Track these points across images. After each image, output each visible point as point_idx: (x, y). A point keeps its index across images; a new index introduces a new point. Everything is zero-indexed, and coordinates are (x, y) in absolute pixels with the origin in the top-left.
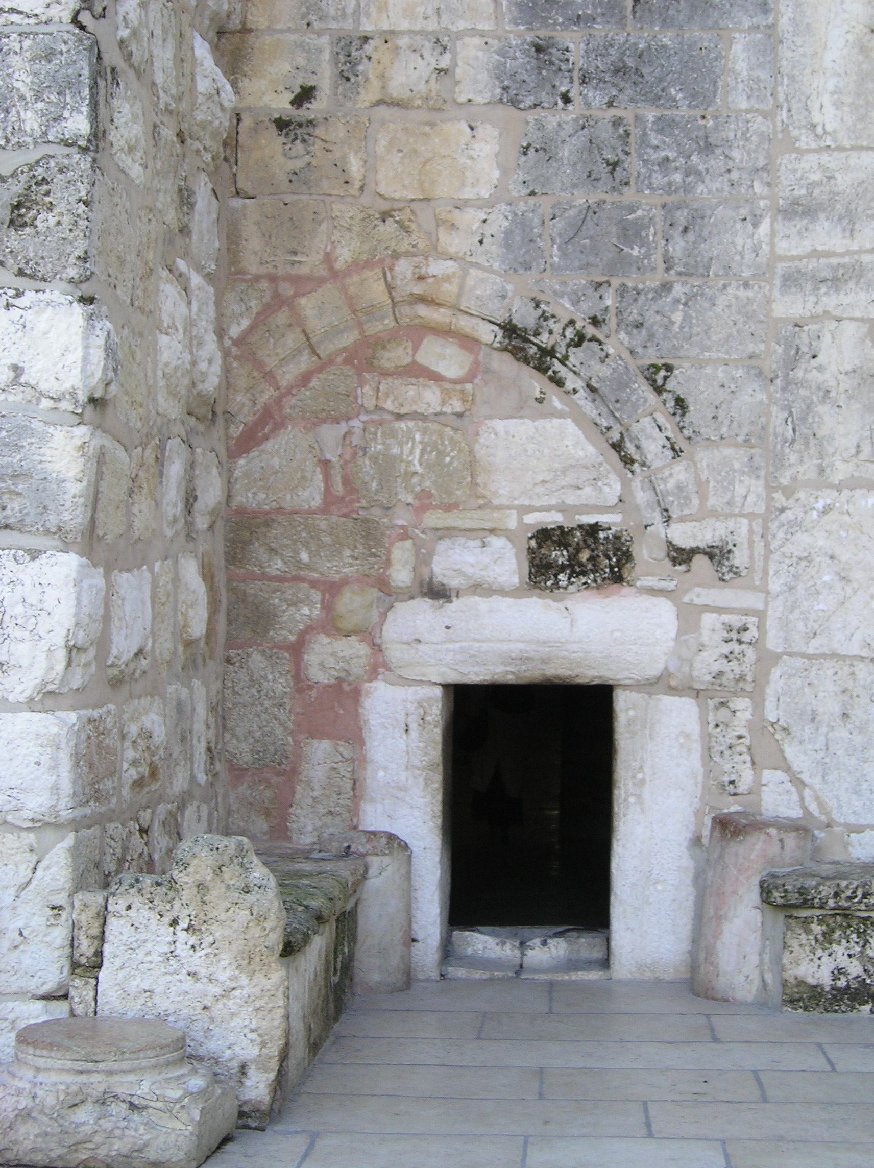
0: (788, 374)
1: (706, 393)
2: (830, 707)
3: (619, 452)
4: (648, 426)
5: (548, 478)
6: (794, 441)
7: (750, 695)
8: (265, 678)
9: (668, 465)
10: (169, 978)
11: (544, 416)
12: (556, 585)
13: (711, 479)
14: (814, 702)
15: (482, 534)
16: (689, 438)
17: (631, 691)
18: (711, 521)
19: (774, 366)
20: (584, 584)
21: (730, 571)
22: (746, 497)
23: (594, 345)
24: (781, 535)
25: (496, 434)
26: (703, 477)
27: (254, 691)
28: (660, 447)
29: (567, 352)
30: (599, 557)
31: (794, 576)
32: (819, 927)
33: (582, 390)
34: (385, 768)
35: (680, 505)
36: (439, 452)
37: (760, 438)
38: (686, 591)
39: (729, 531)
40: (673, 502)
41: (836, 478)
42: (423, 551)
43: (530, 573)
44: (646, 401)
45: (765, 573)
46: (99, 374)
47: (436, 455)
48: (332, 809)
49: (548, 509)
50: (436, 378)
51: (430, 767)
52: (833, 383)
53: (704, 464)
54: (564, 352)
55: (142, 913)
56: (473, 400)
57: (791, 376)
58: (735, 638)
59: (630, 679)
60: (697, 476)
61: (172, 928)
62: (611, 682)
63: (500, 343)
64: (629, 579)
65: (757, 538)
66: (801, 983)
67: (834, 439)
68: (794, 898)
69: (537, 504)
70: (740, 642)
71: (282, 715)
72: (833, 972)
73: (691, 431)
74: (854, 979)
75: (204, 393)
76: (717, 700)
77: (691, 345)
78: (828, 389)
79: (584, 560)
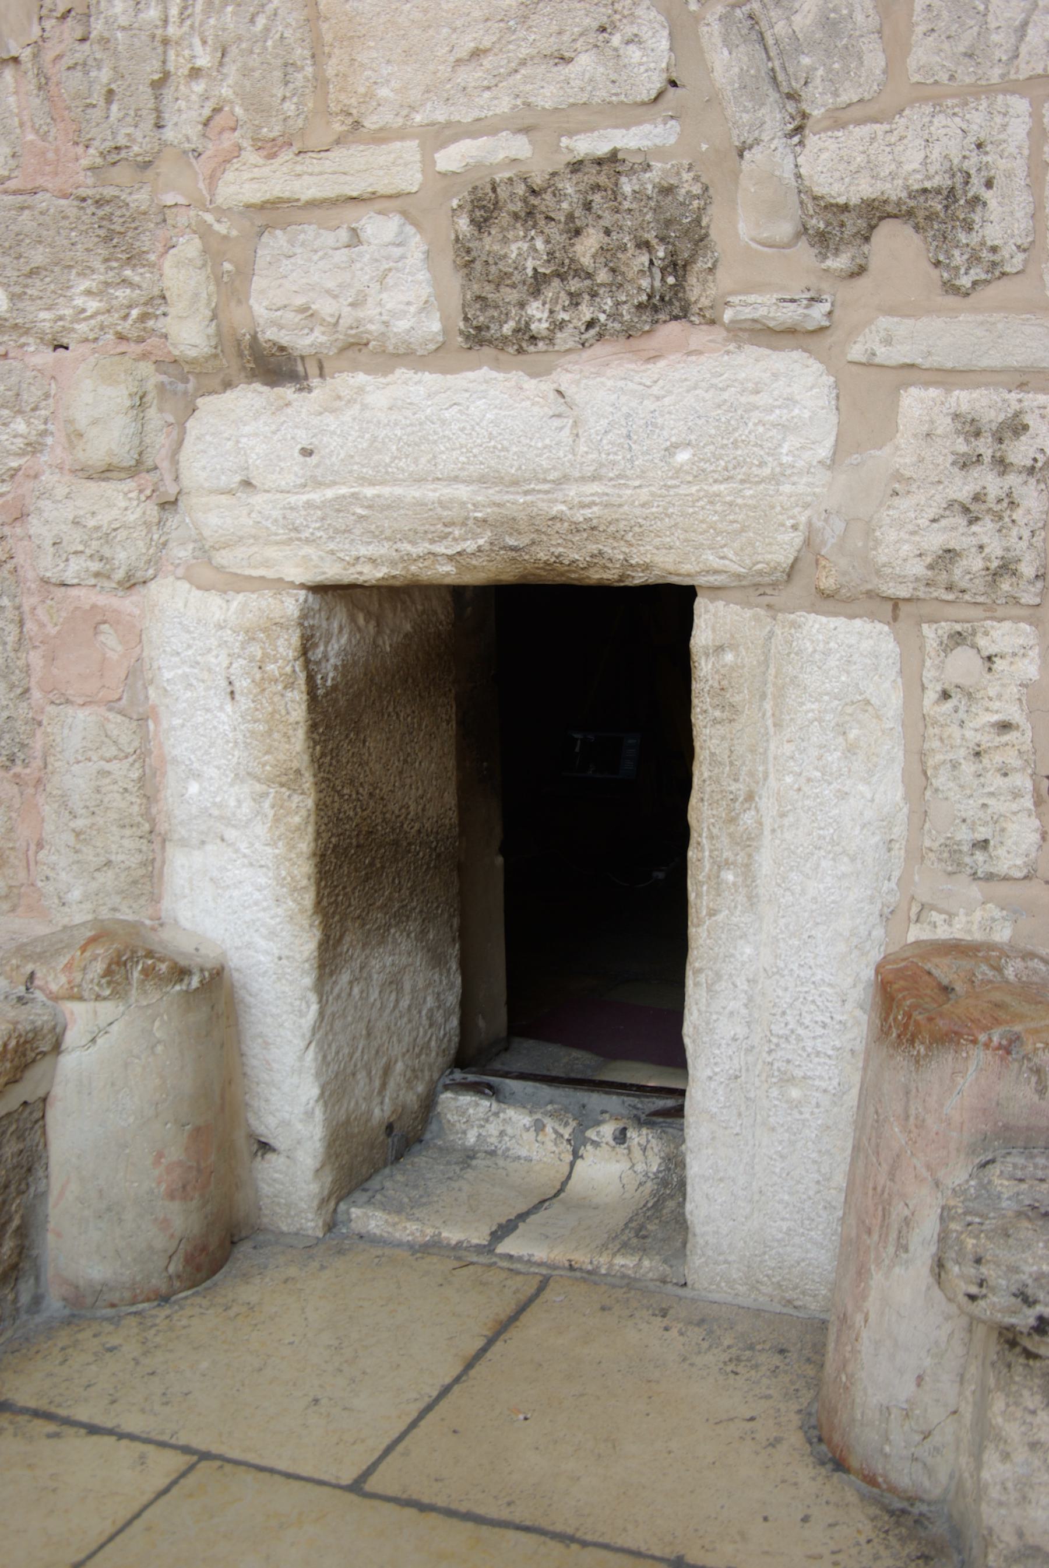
5: (486, 43)
15: (350, 213)
18: (916, 115)
20: (590, 325)
21: (975, 259)
22: (1025, 24)
30: (624, 248)
39: (972, 139)
42: (227, 266)
43: (464, 306)
48: (113, 858)
58: (987, 459)
59: (716, 572)
62: (687, 582)
64: (704, 302)
69: (467, 116)
70: (1002, 465)
76: (945, 627)
79: (586, 261)
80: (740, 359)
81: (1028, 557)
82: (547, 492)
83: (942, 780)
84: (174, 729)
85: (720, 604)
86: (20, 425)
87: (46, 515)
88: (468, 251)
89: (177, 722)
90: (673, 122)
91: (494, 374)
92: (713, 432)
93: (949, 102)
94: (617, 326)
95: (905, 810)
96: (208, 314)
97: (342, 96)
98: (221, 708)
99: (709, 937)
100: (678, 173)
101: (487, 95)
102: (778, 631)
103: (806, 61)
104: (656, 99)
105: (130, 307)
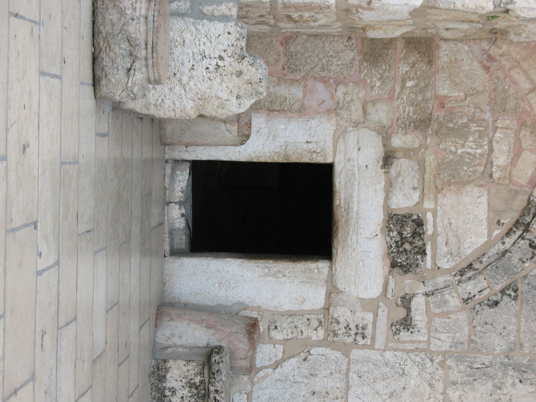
0: (510, 366)
1: (500, 318)
2: (318, 384)
3: (467, 268)
4: (482, 285)
5: (453, 226)
6: (472, 368)
7: (325, 339)
8: (339, 59)
9: (459, 296)
10: (191, 55)
11: (489, 224)
12: (390, 230)
13: (450, 320)
14: (321, 375)
15: (421, 188)
16: (474, 309)
17: (329, 271)
18: (426, 319)
19: (515, 358)
20: (391, 246)
21: (397, 330)
22: (440, 340)
23: (529, 256)
24: (418, 359)
25: (479, 197)
26: (451, 316)
27: (331, 53)
28: (470, 291)
29: (527, 239)
30: (406, 255)
31: (394, 365)
32: (198, 381)
33: (504, 247)
34: (285, 129)
35: (435, 302)
36: (469, 163)
37: (474, 349)
38: (385, 304)
40: (437, 298)
41: (450, 392)
42: (412, 154)
43: (398, 215)
44: (497, 284)
45: (396, 350)
46: (522, 15)
47: (467, 162)
49: (435, 226)
50: (513, 162)
51: (286, 156)
52: (505, 391)
53: (459, 316)
54: (526, 237)
55: (226, 41)
56: (500, 184)
57: (509, 367)
58: (358, 331)
60: (451, 312)
61: (218, 57)
62: (334, 260)
63: (533, 200)
64: (394, 272)
65: (415, 345)
66: (167, 370)
67: (472, 391)
68: (215, 368)
69: (438, 220)
70: (356, 334)
71: (317, 69)
72: (173, 388)
73: (478, 309)
74: (170, 399)
75: (508, 35)
77: (529, 311)
78: (502, 389)
79: (405, 246)
80: (382, 278)
81: (338, 339)
82: (355, 230)
83: (290, 319)
84: (298, 123)
86: (378, 84)
87: (354, 90)
88: (409, 217)
89: (300, 124)
90: (431, 267)
91: (382, 219)
93: (428, 325)
94: (390, 252)
95: (283, 311)
96: (401, 146)
97: (446, 189)
98: (304, 139)
100: (420, 268)
101: (442, 225)
102: (322, 283)
103: (439, 297)
104: (436, 264)
105: (404, 125)
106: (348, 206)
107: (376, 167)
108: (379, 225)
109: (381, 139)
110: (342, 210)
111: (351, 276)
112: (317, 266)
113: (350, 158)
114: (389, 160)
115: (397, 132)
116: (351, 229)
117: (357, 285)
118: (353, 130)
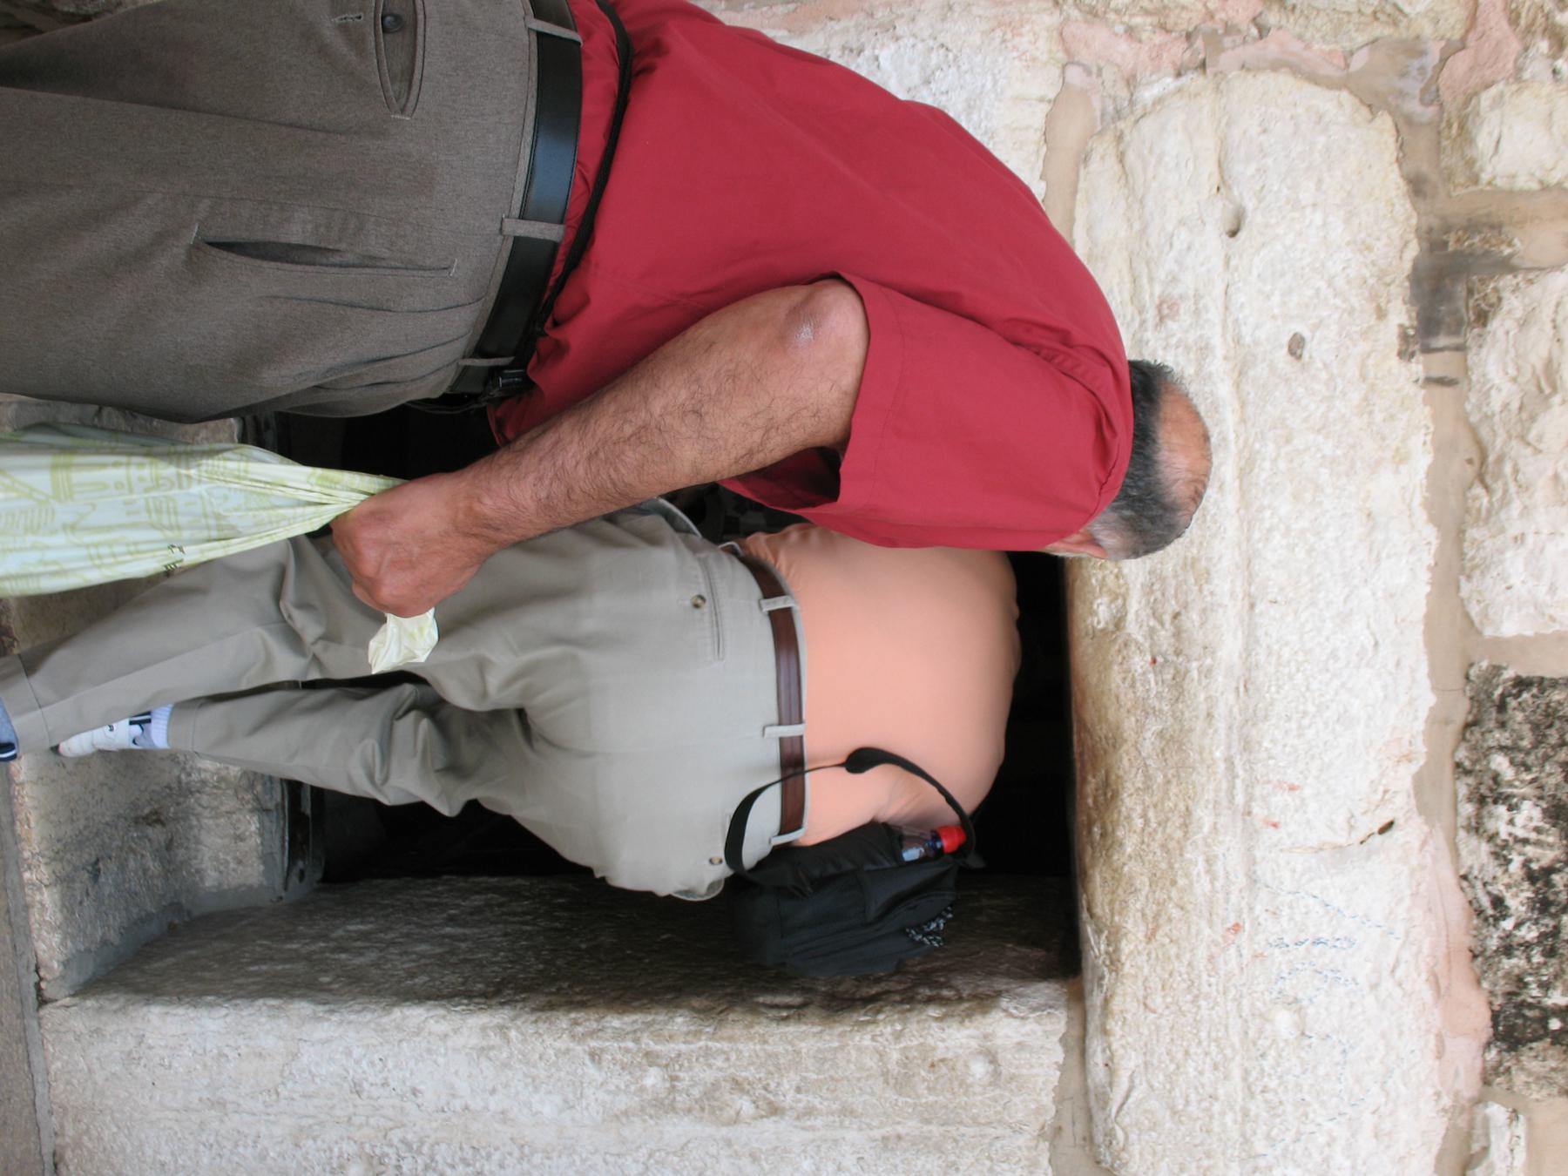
12: (1490, 794)
17: (1063, 1068)
20: (1498, 902)
43: (1543, 684)
64: (1519, 1078)
85: (1059, 1055)
91: (1423, 714)
92: (1321, 1071)
94: (1493, 943)
96: (1554, 178)
99: (558, 1053)
102: (1022, 1140)
106: (1178, 634)
107: (1363, 346)
108: (1408, 758)
109: (1389, 139)
110: (1139, 663)
111: (1217, 1108)
112: (986, 1037)
113: (1176, 292)
114: (1461, 290)
115: (1519, 70)
116: (1209, 795)
117: (1262, 1163)
118: (1179, 90)
